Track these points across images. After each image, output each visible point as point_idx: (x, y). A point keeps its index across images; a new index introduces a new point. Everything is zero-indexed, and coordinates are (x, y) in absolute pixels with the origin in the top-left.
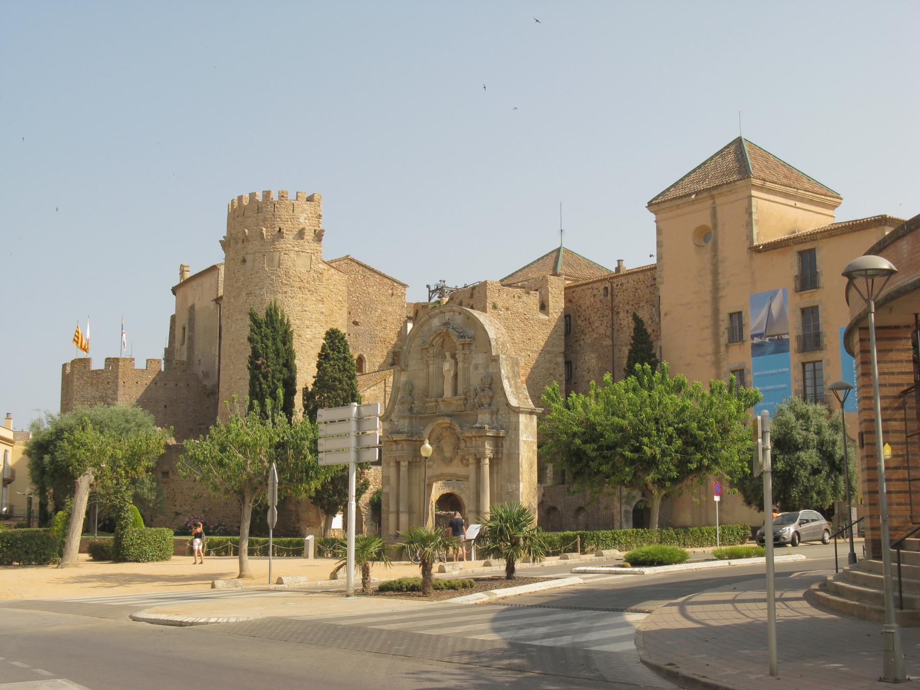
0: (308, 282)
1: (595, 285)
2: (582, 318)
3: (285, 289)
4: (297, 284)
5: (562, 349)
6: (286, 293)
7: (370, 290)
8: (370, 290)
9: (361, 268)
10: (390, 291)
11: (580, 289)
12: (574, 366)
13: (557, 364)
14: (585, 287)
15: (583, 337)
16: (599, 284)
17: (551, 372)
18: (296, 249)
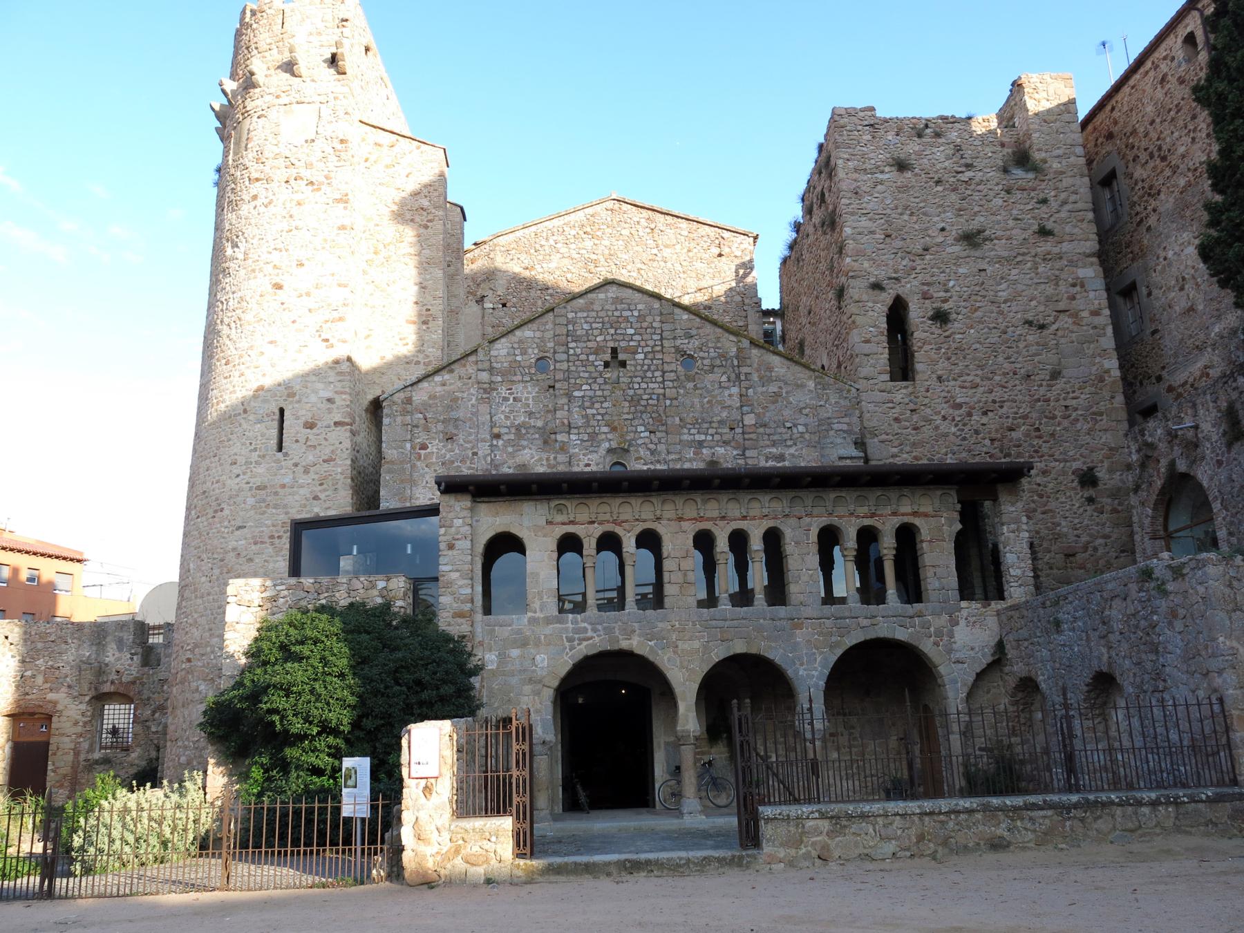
0: (309, 166)
1: (1161, 52)
2: (1144, 157)
3: (253, 192)
4: (280, 175)
5: (1092, 245)
6: (255, 197)
7: (667, 252)
8: (667, 252)
9: (645, 213)
10: (717, 251)
11: (1126, 89)
12: (1144, 291)
13: (1080, 283)
14: (1137, 76)
15: (1153, 203)
16: (1170, 41)
17: (1061, 306)
18: (284, 100)
